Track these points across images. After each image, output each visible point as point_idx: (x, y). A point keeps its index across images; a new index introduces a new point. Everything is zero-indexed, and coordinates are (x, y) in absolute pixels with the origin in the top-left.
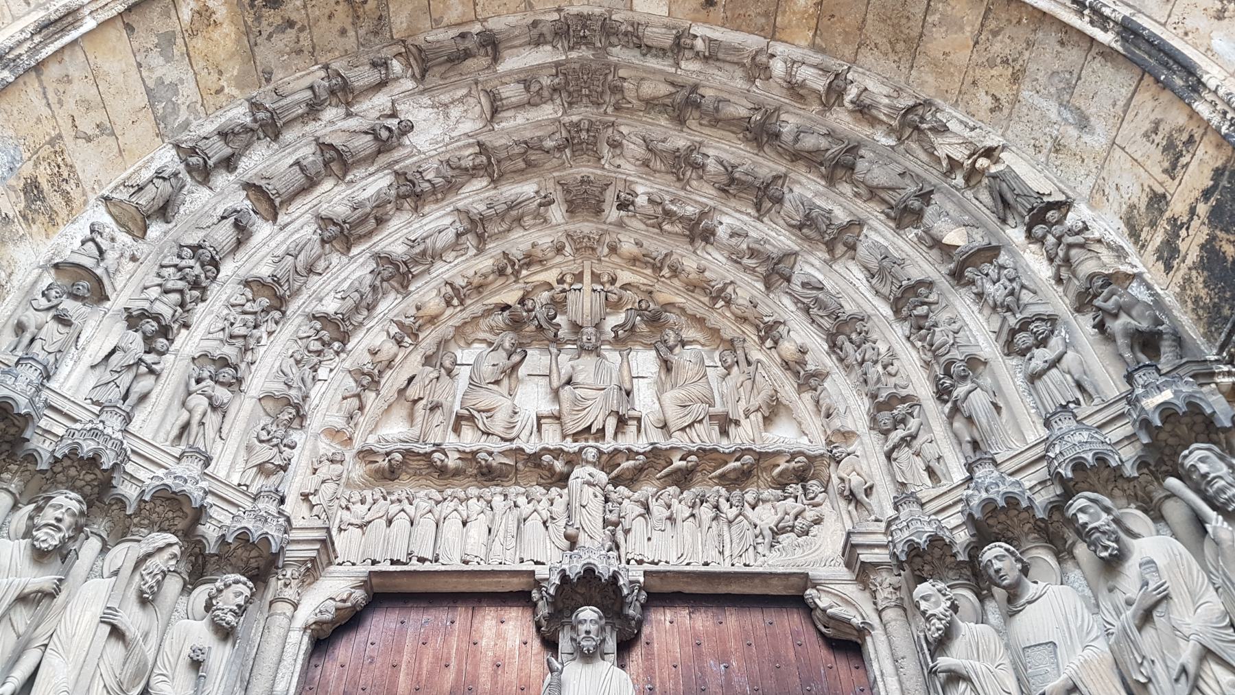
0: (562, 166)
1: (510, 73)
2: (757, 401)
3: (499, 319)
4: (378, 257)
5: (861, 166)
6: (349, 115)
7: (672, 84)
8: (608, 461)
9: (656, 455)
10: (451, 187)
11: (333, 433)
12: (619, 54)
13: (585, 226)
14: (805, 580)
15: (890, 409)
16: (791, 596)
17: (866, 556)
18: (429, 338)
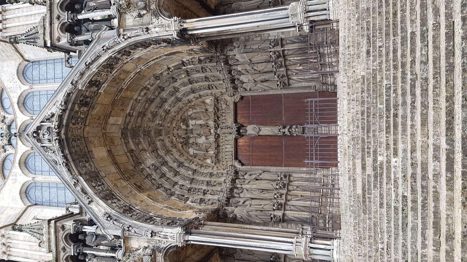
0: (152, 137)
1: (135, 147)
2: (203, 105)
3: (184, 147)
4: (178, 167)
5: (164, 86)
6: (152, 174)
7: (138, 117)
8: (216, 128)
9: (215, 121)
10: (161, 157)
11: (212, 169)
12: (129, 127)
13: (163, 132)
14: (234, 102)
15: (209, 88)
16: (235, 104)
17: (232, 95)
18: (190, 158)
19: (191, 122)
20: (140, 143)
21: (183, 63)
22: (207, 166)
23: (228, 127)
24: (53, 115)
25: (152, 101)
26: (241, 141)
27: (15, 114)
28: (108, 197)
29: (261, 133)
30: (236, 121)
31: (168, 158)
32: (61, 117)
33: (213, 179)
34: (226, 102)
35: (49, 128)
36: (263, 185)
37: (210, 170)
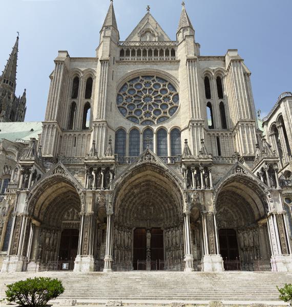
15: (167, 218)
16: (160, 228)
19: (152, 208)
20: (143, 186)
21: (177, 207)
22: (133, 215)
23: (150, 224)
24: (156, 161)
25: (162, 192)
26: (144, 230)
27: (157, 125)
28: (124, 182)
29: (147, 239)
30: (153, 228)
31: (137, 198)
32: (155, 164)
33: (128, 218)
34: (161, 224)
35: (150, 159)
36: (126, 240)
37: (132, 216)
